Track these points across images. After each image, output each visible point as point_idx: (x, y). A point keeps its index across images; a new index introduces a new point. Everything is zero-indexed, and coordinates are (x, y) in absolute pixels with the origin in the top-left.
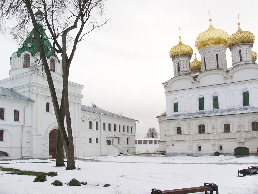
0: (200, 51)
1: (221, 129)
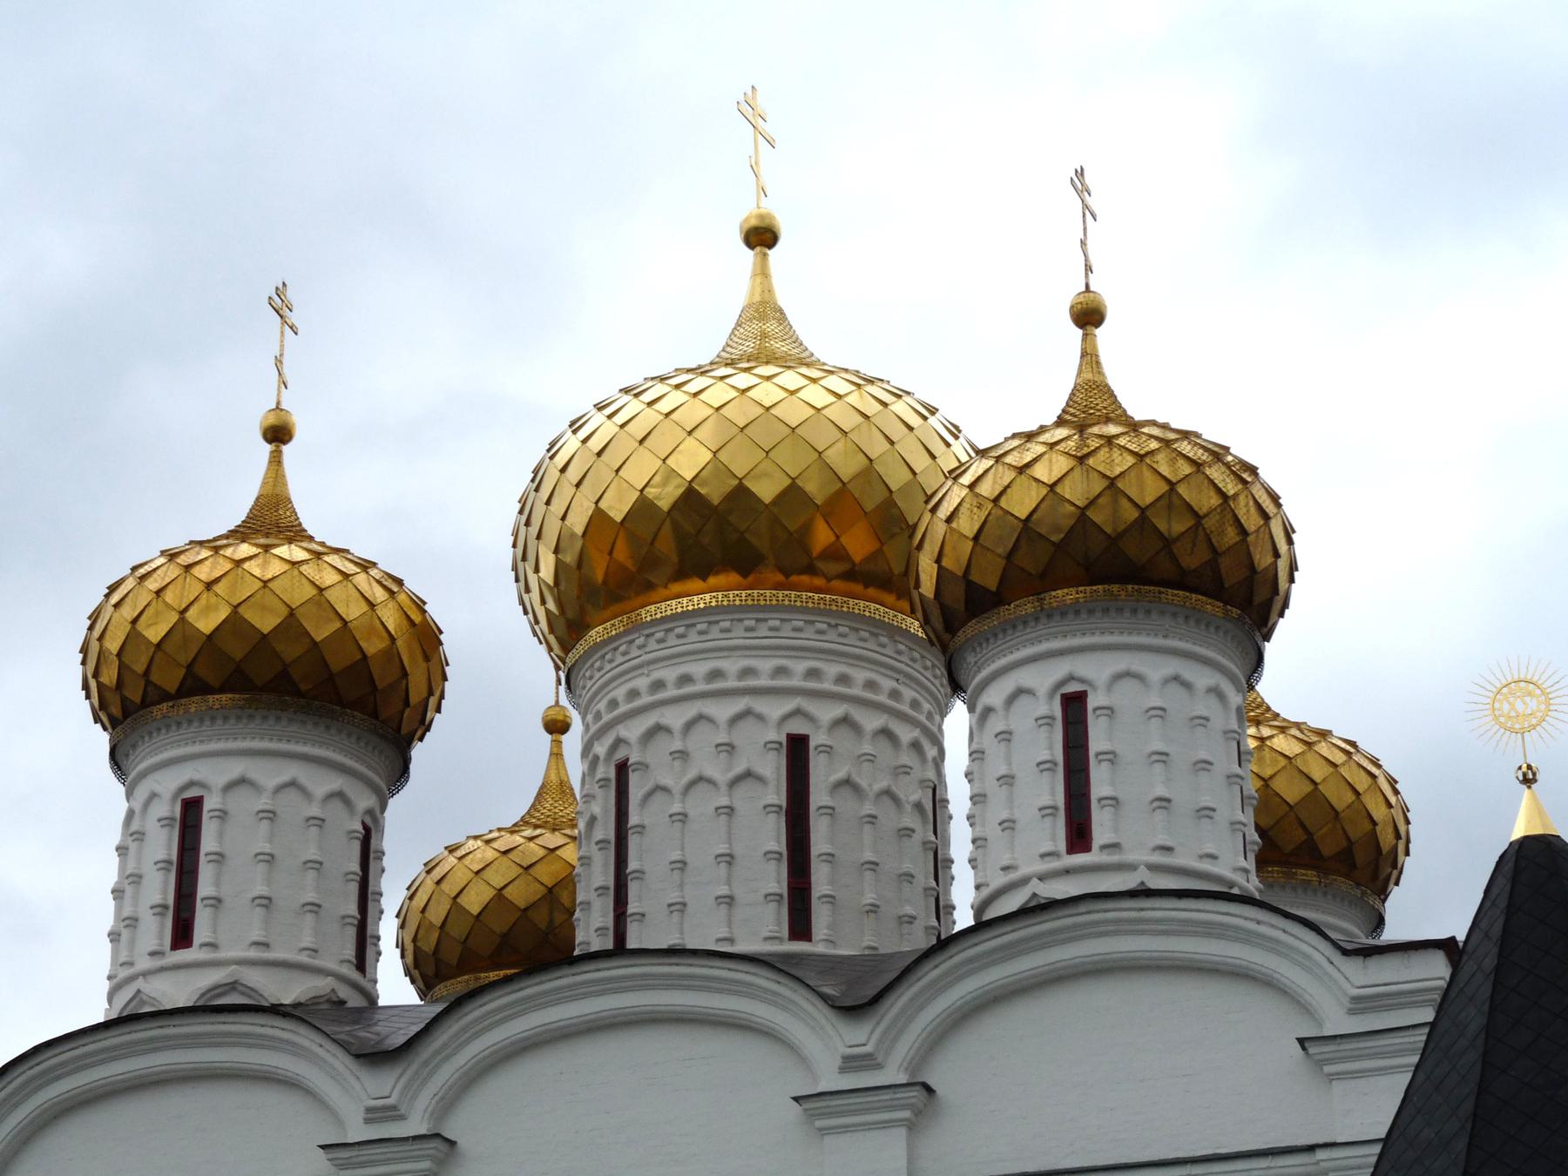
0: (571, 658)
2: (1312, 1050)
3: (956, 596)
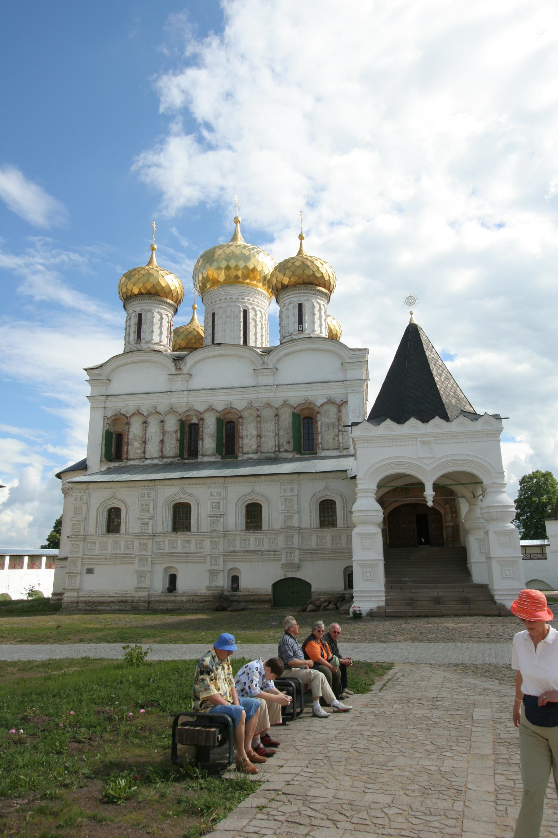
2: (344, 365)
3: (279, 286)
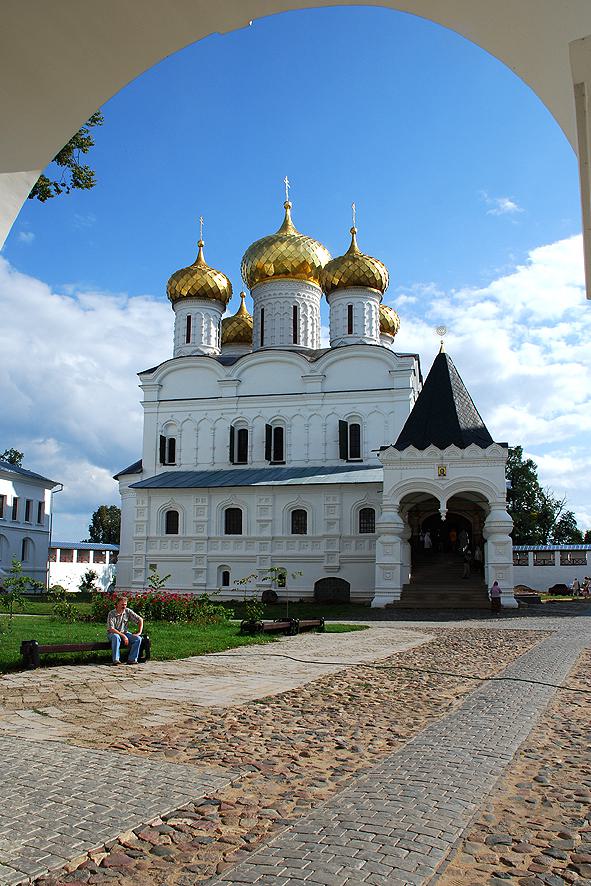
1: (284, 522)
3: (329, 286)
